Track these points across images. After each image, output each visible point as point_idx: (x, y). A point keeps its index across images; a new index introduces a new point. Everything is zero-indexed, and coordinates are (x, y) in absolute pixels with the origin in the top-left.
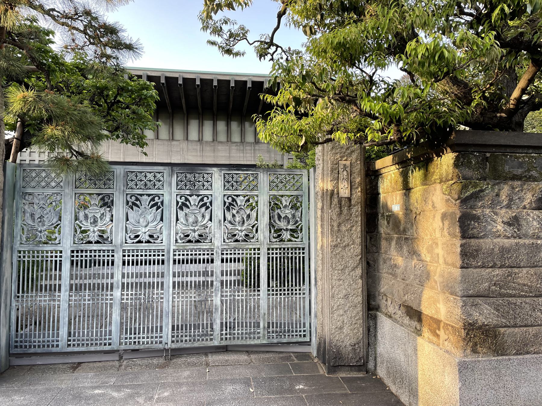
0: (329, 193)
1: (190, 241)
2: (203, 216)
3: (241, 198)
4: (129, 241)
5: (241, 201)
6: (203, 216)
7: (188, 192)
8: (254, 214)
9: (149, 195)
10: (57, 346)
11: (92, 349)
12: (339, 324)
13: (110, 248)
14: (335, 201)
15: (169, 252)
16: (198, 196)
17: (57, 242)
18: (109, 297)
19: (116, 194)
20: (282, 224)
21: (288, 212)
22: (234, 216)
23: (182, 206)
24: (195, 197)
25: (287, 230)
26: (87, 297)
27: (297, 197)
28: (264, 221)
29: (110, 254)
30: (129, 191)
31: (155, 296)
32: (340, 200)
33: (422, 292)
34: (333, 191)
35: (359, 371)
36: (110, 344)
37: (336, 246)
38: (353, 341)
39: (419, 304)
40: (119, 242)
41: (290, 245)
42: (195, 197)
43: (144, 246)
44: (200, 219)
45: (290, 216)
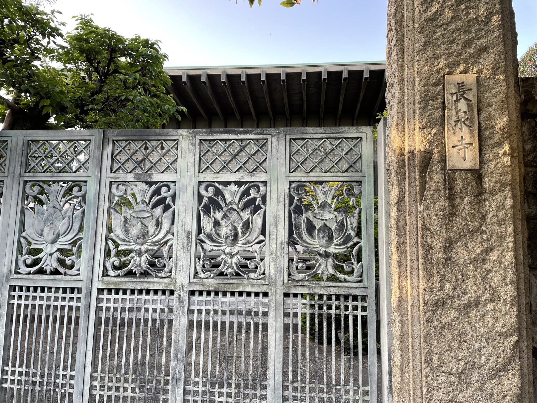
0: (417, 160)
1: (131, 273)
2: (158, 224)
3: (233, 188)
4: (23, 269)
5: (234, 194)
6: (158, 224)
8: (257, 220)
14: (436, 179)
21: (329, 217)
22: (217, 223)
25: (327, 255)
30: (28, 177)
37: (440, 304)
41: (333, 288)
44: (151, 229)
45: (333, 226)
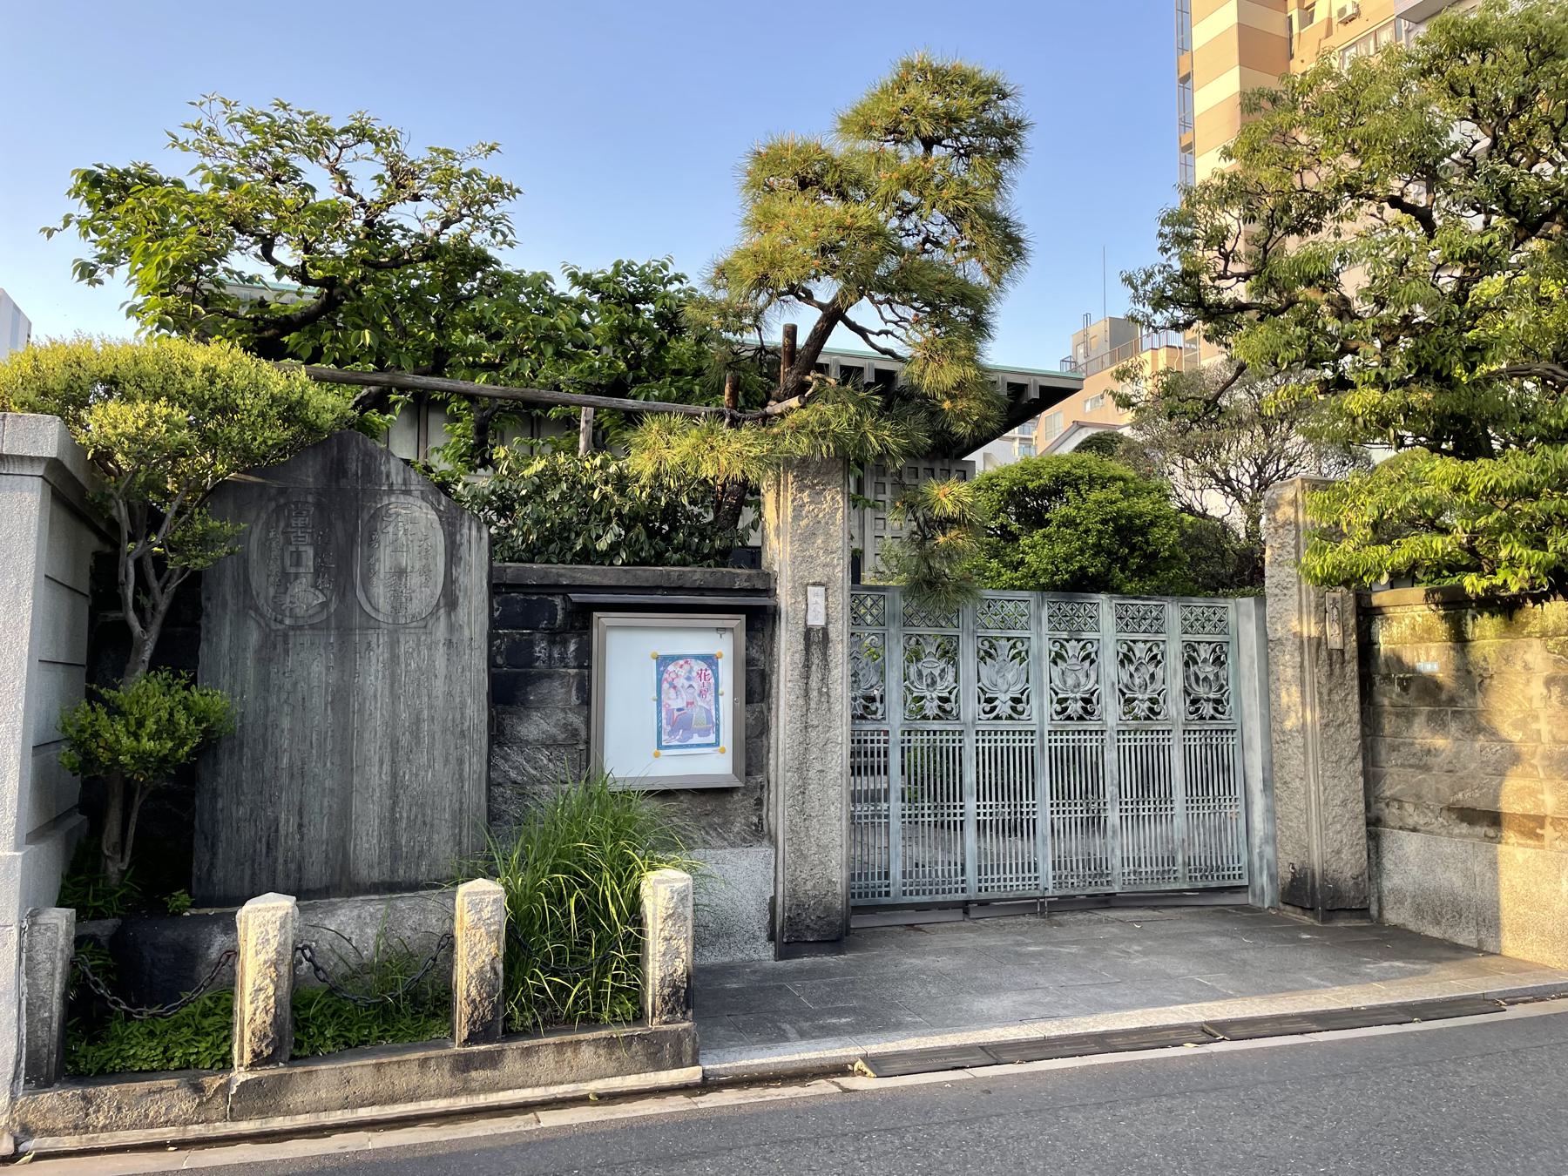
0: (1314, 643)
1: (1069, 718)
2: (1087, 676)
3: (1141, 645)
4: (983, 716)
5: (1141, 650)
6: (1087, 676)
7: (1065, 635)
8: (1159, 673)
9: (1009, 639)
10: (887, 894)
11: (940, 898)
12: (1336, 845)
13: (959, 728)
14: (1324, 654)
15: (1042, 735)
16: (1079, 641)
17: (879, 716)
18: (958, 811)
19: (963, 637)
20: (1201, 691)
21: (1209, 670)
22: (1131, 675)
23: (1058, 658)
24: (1073, 643)
25: (1208, 700)
26: (926, 811)
27: (1220, 644)
28: (1176, 685)
29: (957, 737)
30: (981, 632)
31: (1025, 810)
32: (1330, 653)
33: (1500, 784)
34: (1319, 639)
35: (1362, 918)
36: (963, 890)
37: (1327, 725)
38: (1356, 871)
39: (1496, 798)
40: (970, 717)
41: (1214, 725)
42: (1073, 643)
43: (1004, 725)
44: (1083, 680)
45: (1212, 677)
